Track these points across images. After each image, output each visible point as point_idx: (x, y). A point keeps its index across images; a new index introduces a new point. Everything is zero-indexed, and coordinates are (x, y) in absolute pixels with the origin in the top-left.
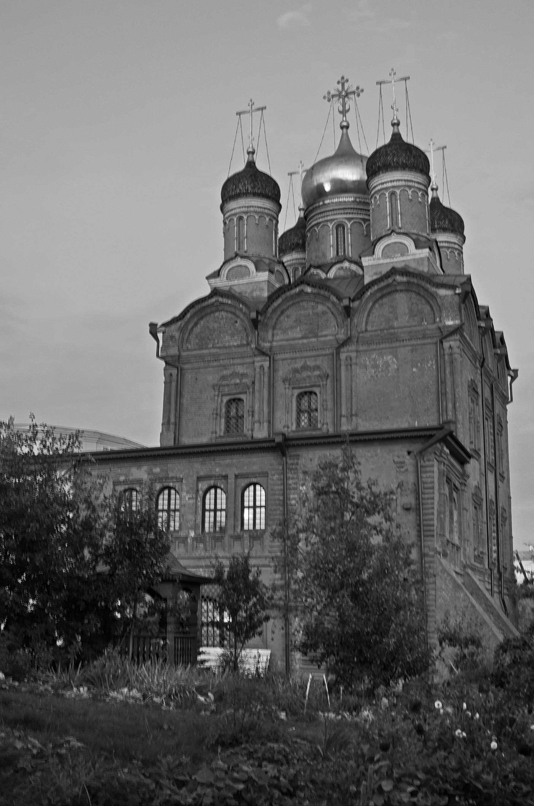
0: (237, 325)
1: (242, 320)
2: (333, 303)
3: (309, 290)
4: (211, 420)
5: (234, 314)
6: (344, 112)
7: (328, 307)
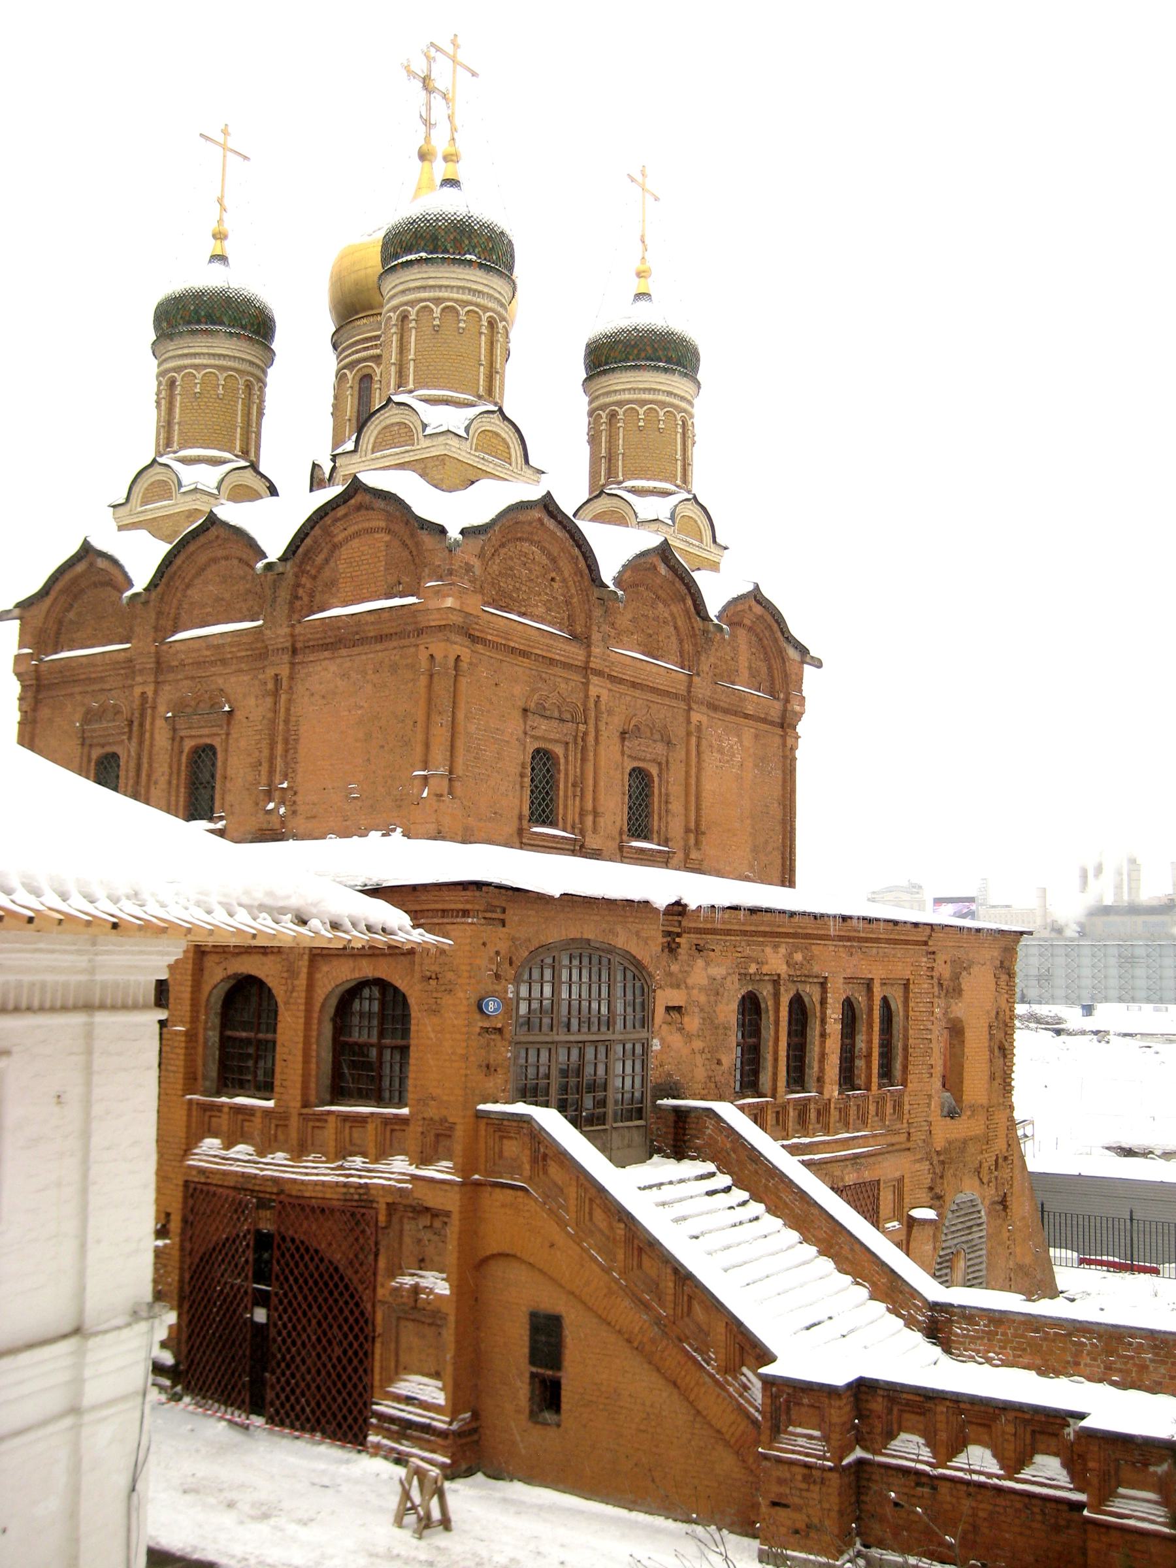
0: (556, 585)
1: (564, 580)
2: (687, 611)
3: (663, 569)
4: (518, 787)
5: (554, 560)
6: (427, 123)
7: (672, 614)
